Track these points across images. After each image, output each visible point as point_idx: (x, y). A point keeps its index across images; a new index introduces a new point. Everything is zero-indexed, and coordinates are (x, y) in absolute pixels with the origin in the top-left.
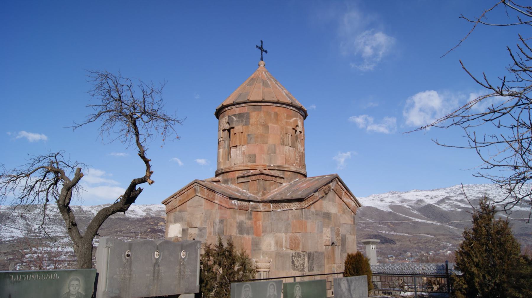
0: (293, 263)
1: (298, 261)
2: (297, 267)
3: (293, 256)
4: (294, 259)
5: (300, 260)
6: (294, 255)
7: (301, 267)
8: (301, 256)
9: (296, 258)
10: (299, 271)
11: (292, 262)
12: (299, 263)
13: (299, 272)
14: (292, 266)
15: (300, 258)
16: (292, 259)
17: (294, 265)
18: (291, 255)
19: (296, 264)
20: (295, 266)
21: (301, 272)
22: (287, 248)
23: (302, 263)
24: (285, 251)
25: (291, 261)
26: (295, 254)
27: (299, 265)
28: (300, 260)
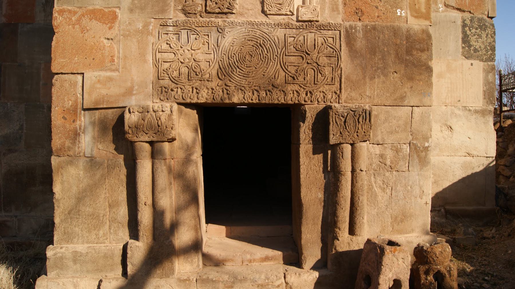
0: (465, 40)
1: (480, 36)
2: (476, 50)
3: (464, 26)
4: (468, 33)
5: (484, 36)
6: (468, 22)
7: (487, 51)
8: (486, 27)
9: (474, 31)
10: (482, 60)
11: (463, 39)
12: (483, 42)
13: (482, 64)
14: (463, 48)
15: (485, 30)
16: (464, 33)
17: (470, 46)
18: (459, 23)
19: (475, 43)
20: (472, 48)
21: (486, 63)
22: (446, 6)
23: (490, 43)
24: (443, 12)
25: (461, 36)
26: (471, 21)
27: (483, 47)
28: (484, 36)
